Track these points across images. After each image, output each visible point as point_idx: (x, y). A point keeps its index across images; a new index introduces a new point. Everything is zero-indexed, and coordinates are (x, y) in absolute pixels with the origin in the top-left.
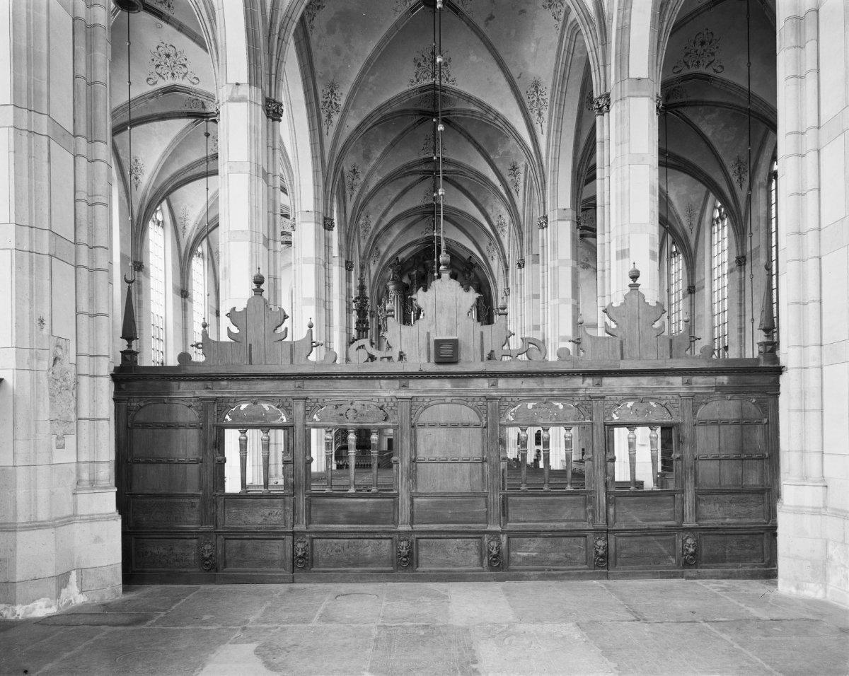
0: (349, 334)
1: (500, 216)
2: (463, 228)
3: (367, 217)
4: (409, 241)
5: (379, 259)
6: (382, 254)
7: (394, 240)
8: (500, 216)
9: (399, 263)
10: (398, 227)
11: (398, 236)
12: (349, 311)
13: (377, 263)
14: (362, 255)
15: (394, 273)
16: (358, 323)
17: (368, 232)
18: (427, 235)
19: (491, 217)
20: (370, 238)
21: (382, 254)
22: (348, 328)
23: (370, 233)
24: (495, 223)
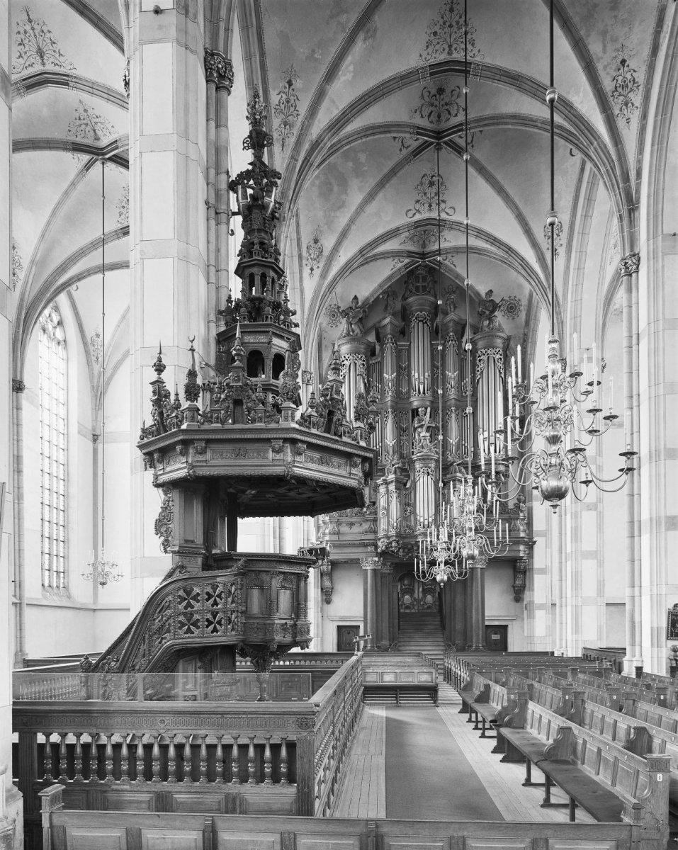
0: (217, 287)
1: (623, 62)
2: (498, 182)
3: (290, 83)
4: (381, 231)
5: (321, 265)
7: (352, 221)
8: (623, 62)
10: (360, 189)
11: (361, 208)
16: (247, 249)
17: (292, 126)
18: (418, 217)
19: (599, 66)
20: (298, 143)
21: (326, 253)
22: (213, 268)
23: (296, 131)
24: (608, 85)
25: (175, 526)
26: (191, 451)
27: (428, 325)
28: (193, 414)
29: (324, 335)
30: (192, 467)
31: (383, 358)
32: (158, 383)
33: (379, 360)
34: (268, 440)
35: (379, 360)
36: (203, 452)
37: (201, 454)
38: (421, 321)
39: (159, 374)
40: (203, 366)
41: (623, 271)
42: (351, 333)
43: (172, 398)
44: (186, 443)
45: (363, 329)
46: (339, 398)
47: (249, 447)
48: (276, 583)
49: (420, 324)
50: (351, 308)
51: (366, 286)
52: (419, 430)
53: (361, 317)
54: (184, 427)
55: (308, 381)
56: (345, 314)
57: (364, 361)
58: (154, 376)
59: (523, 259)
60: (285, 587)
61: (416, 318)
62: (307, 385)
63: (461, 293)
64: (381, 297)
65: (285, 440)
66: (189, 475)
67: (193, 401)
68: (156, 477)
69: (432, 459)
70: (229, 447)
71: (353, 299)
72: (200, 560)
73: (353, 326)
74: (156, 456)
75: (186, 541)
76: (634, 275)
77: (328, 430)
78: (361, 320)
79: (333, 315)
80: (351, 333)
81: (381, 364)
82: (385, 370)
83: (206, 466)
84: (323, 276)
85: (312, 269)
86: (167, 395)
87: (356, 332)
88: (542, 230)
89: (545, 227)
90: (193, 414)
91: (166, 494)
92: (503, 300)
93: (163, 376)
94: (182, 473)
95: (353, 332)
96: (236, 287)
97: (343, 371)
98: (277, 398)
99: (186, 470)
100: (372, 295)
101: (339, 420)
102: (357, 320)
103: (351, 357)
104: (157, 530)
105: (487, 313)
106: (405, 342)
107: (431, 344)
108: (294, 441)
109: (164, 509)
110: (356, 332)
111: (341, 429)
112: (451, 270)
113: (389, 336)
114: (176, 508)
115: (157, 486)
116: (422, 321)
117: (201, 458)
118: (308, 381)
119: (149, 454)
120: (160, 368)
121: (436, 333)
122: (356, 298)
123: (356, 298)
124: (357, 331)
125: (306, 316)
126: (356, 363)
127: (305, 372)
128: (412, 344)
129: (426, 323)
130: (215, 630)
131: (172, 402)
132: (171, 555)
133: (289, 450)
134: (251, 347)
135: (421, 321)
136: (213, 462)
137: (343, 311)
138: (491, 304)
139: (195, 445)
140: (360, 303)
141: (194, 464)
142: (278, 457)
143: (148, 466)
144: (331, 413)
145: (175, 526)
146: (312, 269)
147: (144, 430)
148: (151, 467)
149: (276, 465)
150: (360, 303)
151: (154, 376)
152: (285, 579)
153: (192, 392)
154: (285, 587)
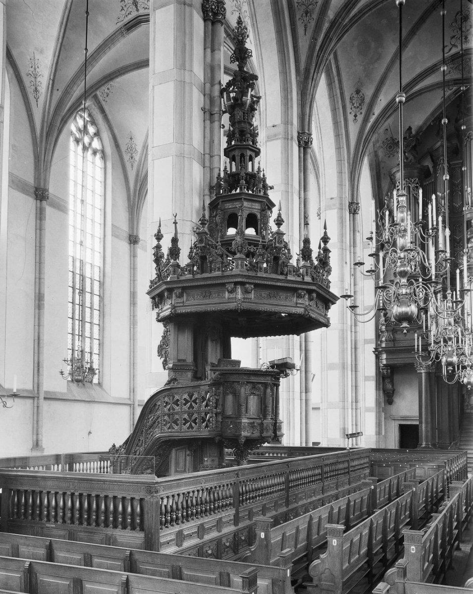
5: (364, 111)
9: (414, 136)
12: (209, 114)
13: (360, 118)
14: (303, 66)
21: (367, 100)
25: (171, 350)
26: (174, 295)
28: (175, 269)
29: (382, 165)
30: (174, 307)
32: (158, 247)
33: (433, 180)
34: (223, 285)
36: (180, 296)
37: (179, 297)
39: (159, 241)
40: (195, 230)
43: (166, 257)
44: (170, 291)
45: (416, 156)
46: (282, 245)
47: (213, 290)
48: (244, 391)
54: (169, 279)
55: (355, 211)
57: (417, 183)
58: (155, 243)
60: (253, 394)
62: (353, 214)
65: (236, 283)
66: (172, 313)
67: (175, 260)
68: (158, 314)
70: (198, 291)
71: (408, 129)
72: (190, 375)
73: (406, 154)
74: (157, 300)
75: (179, 361)
77: (276, 273)
78: (414, 148)
82: (438, 189)
83: (182, 306)
84: (366, 120)
85: (356, 116)
86: (162, 256)
87: (410, 159)
90: (175, 269)
91: (165, 326)
93: (161, 242)
94: (167, 313)
96: (223, 163)
98: (249, 247)
99: (170, 310)
100: (425, 123)
101: (283, 263)
104: (160, 353)
108: (242, 284)
109: (164, 337)
110: (410, 159)
111: (286, 269)
114: (172, 337)
115: (159, 321)
117: (180, 300)
119: (153, 298)
120: (159, 237)
122: (410, 128)
123: (410, 128)
125: (352, 156)
127: (352, 203)
130: (191, 427)
131: (165, 261)
132: (168, 371)
133: (239, 290)
134: (230, 211)
136: (187, 303)
139: (175, 291)
140: (414, 132)
141: (176, 305)
142: (231, 296)
143: (154, 307)
144: (276, 259)
145: (171, 350)
146: (356, 116)
147: (152, 282)
148: (156, 308)
149: (231, 302)
150: (414, 132)
151: (155, 243)
152: (254, 388)
153: (175, 252)
154: (253, 394)
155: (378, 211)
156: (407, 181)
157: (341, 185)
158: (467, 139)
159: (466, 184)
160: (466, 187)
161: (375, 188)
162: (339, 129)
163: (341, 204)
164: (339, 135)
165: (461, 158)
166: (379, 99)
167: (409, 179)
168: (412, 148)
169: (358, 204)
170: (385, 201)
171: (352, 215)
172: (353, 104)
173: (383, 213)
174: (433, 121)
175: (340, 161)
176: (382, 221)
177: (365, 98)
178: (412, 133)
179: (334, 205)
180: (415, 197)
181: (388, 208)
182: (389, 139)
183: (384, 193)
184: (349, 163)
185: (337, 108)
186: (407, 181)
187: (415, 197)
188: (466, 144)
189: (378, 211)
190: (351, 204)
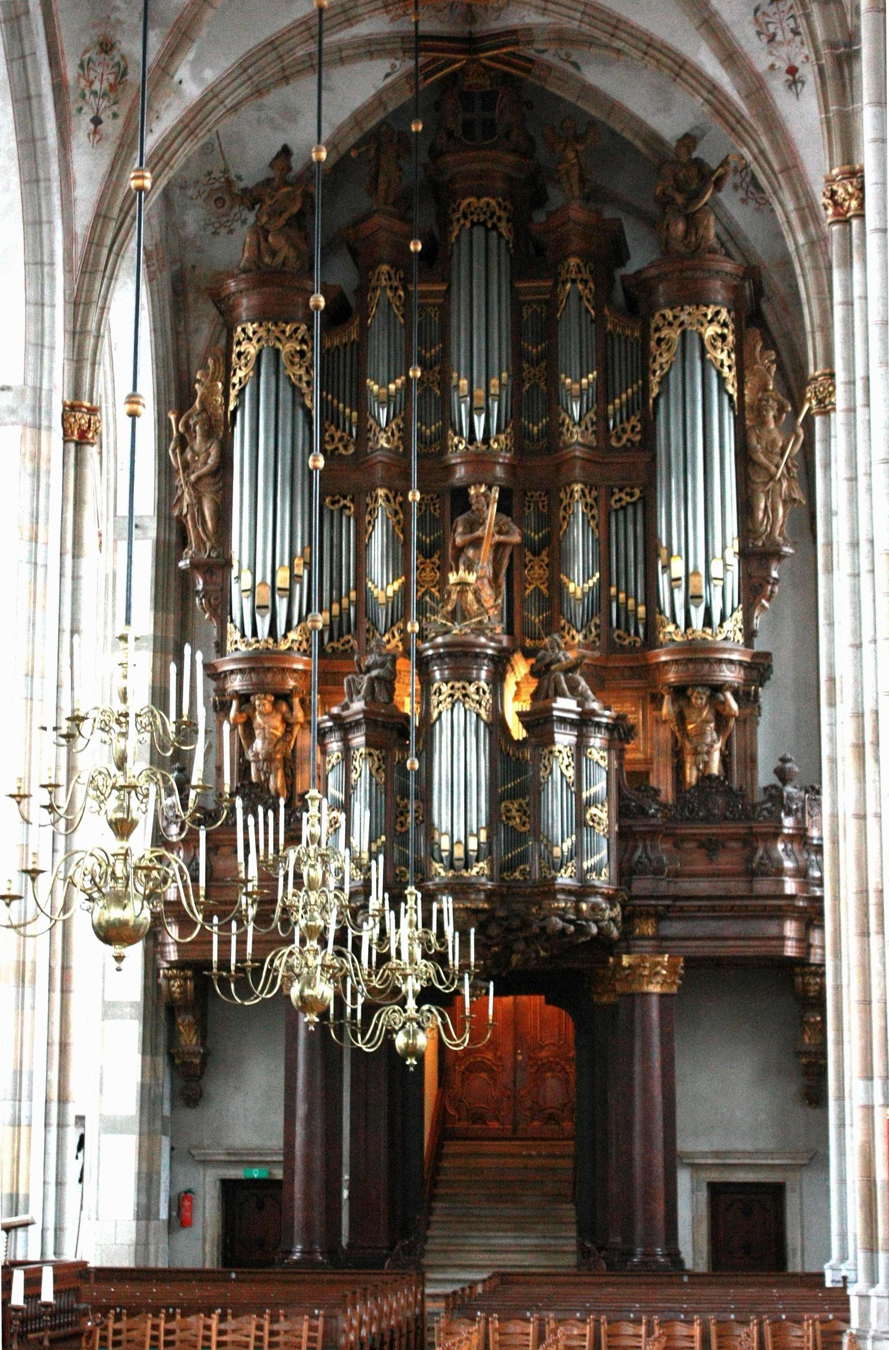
6: (134, 76)
13: (112, 128)
15: (262, 232)
27: (500, 236)
31: (364, 330)
33: (354, 336)
35: (354, 336)
38: (478, 223)
41: (830, 211)
42: (267, 260)
49: (479, 232)
50: (269, 181)
51: (318, 118)
52: (470, 553)
53: (295, 209)
55: (83, 434)
56: (251, 198)
59: (714, 88)
61: (465, 216)
62: (78, 444)
63: (604, 138)
64: (353, 154)
69: (477, 655)
71: (278, 156)
73: (270, 239)
76: (855, 223)
79: (219, 202)
80: (267, 260)
81: (360, 349)
82: (370, 371)
87: (279, 259)
88: (751, 17)
89: (756, 10)
92: (725, 163)
95: (274, 254)
97: (240, 374)
102: (281, 221)
103: (262, 332)
105: (680, 199)
106: (435, 282)
107: (513, 291)
112: (564, 78)
113: (385, 268)
116: (484, 224)
118: (83, 434)
121: (532, 256)
123: (286, 151)
124: (286, 251)
125: (79, 249)
126: (277, 352)
128: (454, 288)
129: (495, 227)
135: (478, 223)
137: (245, 190)
138: (694, 172)
155: (172, 417)
156: (268, 330)
157: (38, 345)
158: (462, 221)
159: (455, 368)
160: (455, 375)
161: (163, 332)
162: (40, 161)
163: (37, 409)
164: (37, 181)
165: (446, 279)
166: (176, 78)
167: (276, 325)
168: (288, 224)
169: (93, 411)
170: (197, 386)
171: (72, 446)
172: (91, 83)
173: (187, 426)
174: (356, 146)
175: (37, 264)
176: (182, 452)
177: (130, 71)
178: (290, 169)
179: (13, 411)
180: (293, 386)
181: (204, 409)
182: (217, 174)
183: (195, 362)
184: (68, 270)
185: (33, 92)
186: (268, 330)
187: (293, 386)
188: (458, 238)
189: (172, 417)
190: (71, 409)
